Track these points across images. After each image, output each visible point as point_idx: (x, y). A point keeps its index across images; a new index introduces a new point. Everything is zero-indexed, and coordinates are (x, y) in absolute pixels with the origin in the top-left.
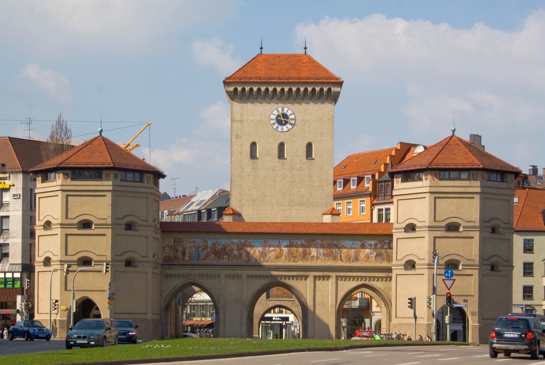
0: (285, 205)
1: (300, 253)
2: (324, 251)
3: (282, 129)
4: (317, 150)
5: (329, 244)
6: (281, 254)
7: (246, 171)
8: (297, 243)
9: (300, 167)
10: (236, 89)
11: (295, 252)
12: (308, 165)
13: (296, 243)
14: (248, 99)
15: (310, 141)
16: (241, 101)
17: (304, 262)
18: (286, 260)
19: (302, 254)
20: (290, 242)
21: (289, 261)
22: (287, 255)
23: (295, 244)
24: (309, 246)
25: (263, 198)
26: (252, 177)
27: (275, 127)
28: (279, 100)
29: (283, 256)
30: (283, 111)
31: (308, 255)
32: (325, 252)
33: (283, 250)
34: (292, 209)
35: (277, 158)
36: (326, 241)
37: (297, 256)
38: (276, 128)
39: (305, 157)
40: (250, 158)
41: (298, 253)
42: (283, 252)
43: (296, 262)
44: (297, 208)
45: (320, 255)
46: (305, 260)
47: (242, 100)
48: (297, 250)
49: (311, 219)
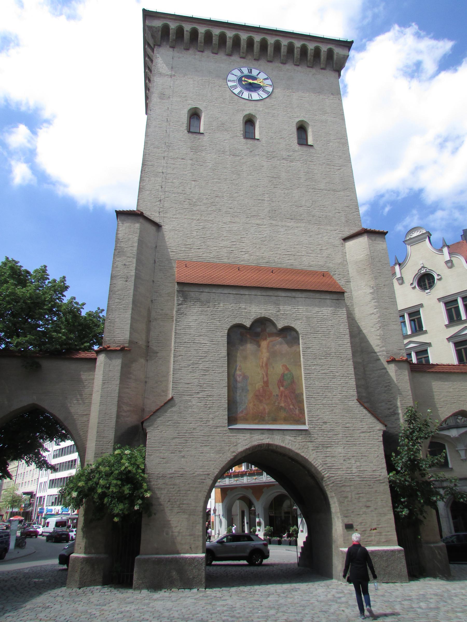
0: (262, 217)
3: (250, 96)
4: (317, 133)
7: (177, 151)
9: (288, 156)
10: (166, 29)
12: (303, 154)
14: (187, 49)
15: (302, 119)
16: (173, 50)
25: (212, 200)
26: (190, 162)
27: (236, 91)
28: (242, 59)
30: (250, 71)
34: (277, 226)
35: (242, 137)
38: (239, 93)
39: (296, 141)
40: (186, 132)
44: (288, 224)
47: (175, 49)
49: (320, 246)
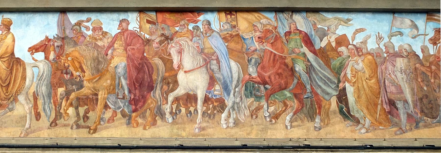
1: (113, 78)
2: (245, 69)
5: (268, 31)
6: (13, 89)
8: (101, 28)
11: (88, 74)
13: (94, 30)
17: (141, 128)
18: (38, 116)
19: (124, 82)
20: (62, 26)
21: (54, 124)
22: (44, 89)
23: (90, 33)
24: (161, 42)
29: (21, 98)
31: (158, 92)
32: (254, 75)
33: (24, 64)
36: (251, 17)
37: (101, 95)
41: (106, 82)
42: (24, 78)
43: (95, 131)
45: (226, 89)
46: (144, 117)
48: (99, 62)
